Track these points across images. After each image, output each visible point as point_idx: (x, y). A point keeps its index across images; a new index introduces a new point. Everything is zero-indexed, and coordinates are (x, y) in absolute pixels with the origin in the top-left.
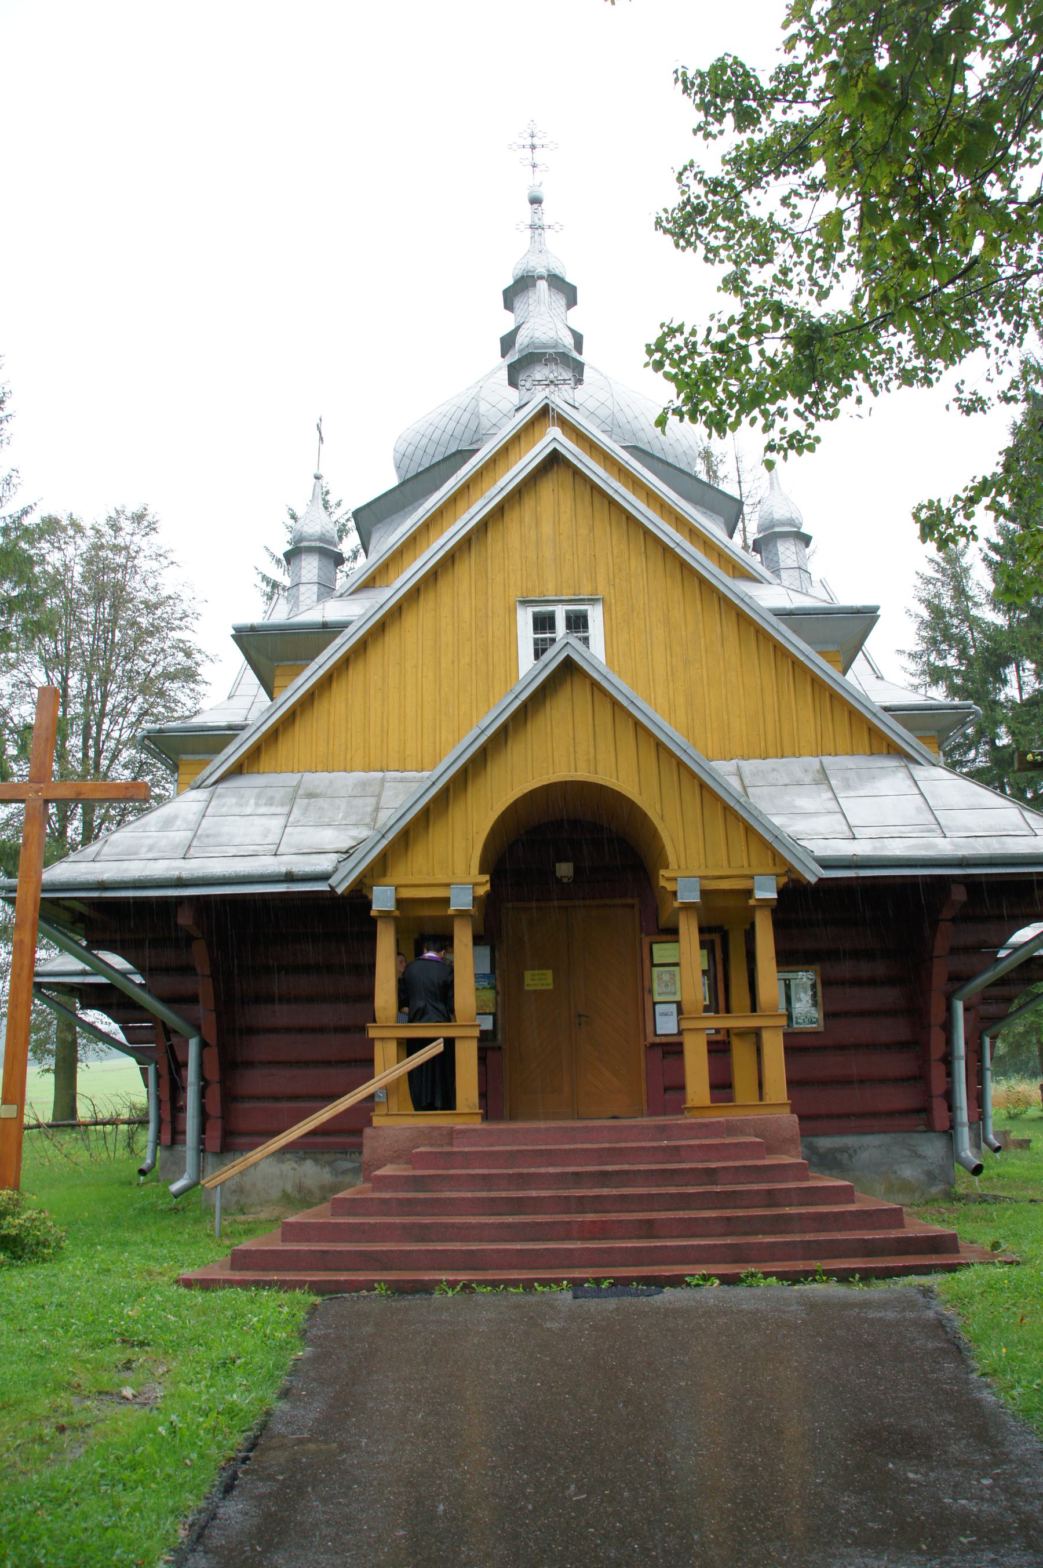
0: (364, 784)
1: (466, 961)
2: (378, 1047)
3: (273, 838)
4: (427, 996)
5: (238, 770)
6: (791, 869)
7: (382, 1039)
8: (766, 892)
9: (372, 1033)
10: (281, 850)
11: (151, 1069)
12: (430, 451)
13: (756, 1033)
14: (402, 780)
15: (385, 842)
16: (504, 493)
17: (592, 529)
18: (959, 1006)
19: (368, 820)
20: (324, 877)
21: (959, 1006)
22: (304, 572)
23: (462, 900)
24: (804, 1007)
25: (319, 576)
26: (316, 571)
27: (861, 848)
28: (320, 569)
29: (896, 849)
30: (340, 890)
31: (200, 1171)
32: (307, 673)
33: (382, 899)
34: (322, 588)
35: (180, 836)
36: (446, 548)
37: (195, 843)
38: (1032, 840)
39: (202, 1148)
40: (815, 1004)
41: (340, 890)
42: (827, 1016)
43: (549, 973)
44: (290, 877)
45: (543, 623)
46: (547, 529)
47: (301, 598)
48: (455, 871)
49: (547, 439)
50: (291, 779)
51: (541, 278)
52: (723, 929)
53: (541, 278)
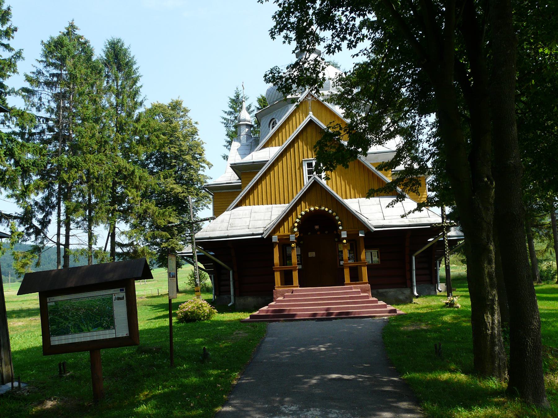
3: (248, 224)
11: (212, 276)
18: (414, 258)
20: (262, 234)
21: (414, 258)
23: (293, 238)
24: (376, 259)
32: (252, 181)
33: (275, 238)
35: (226, 225)
38: (429, 219)
43: (314, 253)
44: (253, 235)
48: (291, 231)
49: (309, 116)
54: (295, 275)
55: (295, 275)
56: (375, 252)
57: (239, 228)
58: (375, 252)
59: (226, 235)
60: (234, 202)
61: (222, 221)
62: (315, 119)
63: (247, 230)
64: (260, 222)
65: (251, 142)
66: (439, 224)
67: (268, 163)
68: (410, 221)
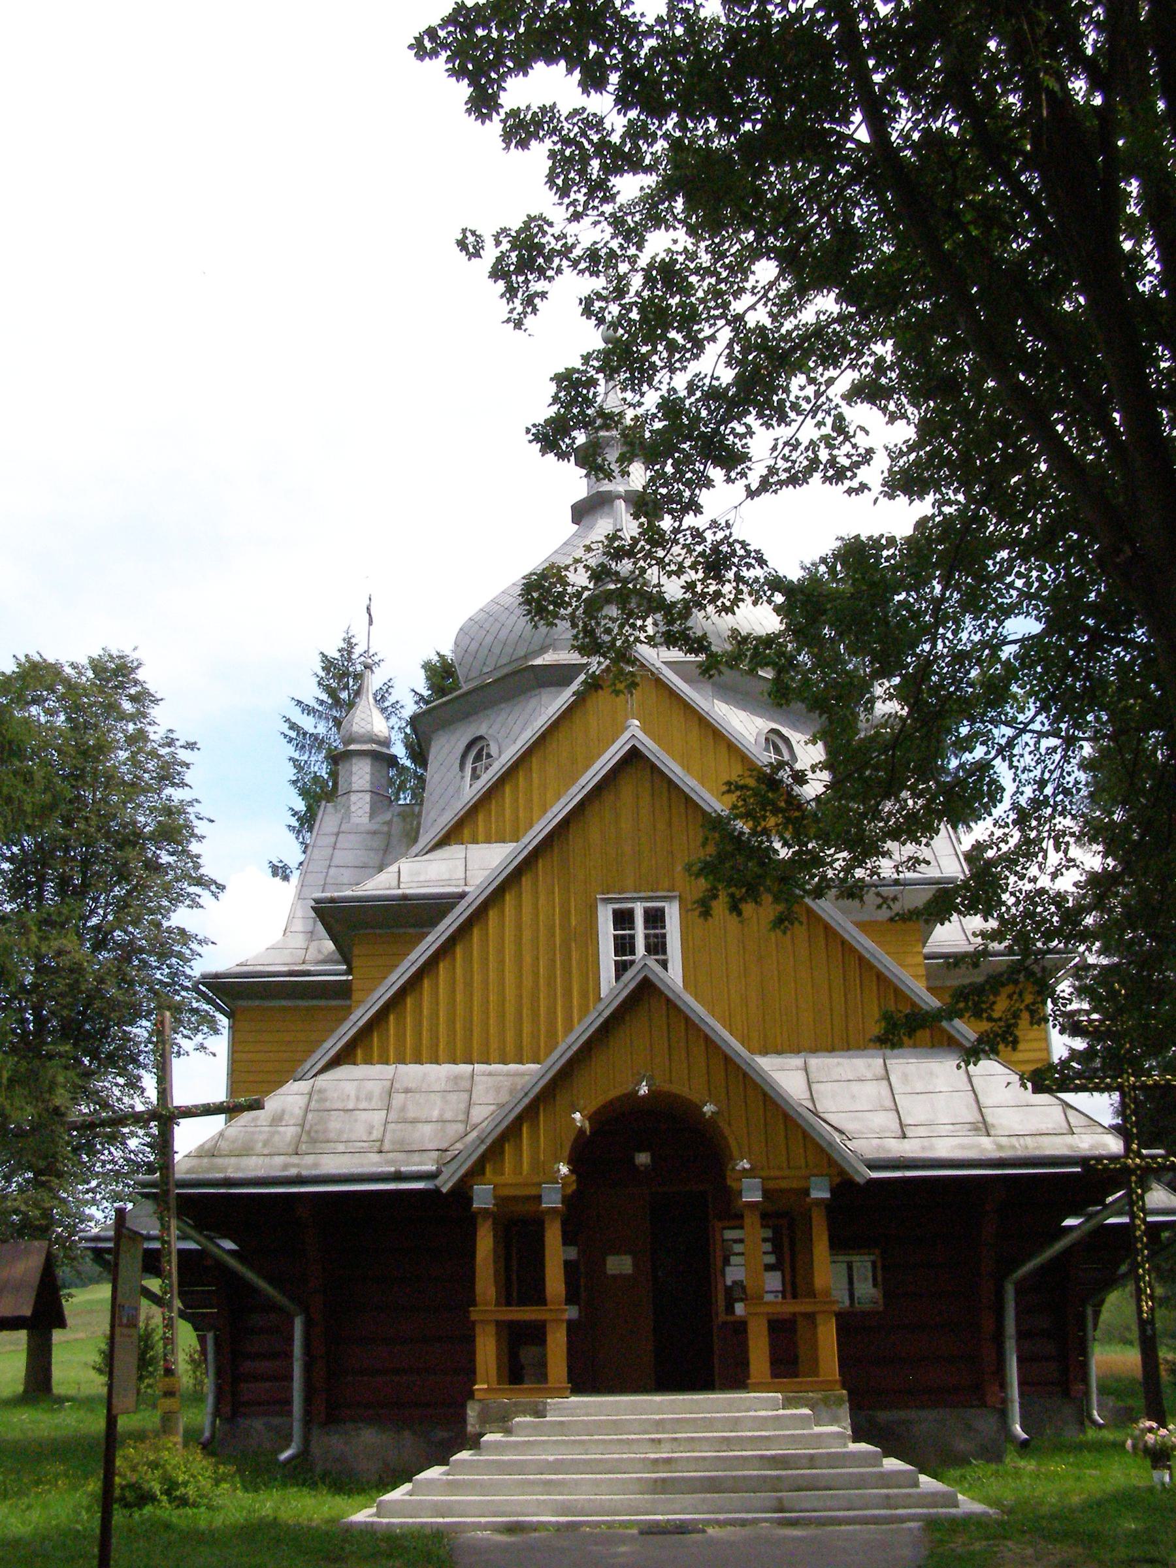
0: (456, 1078)
1: (556, 1253)
2: (478, 1330)
3: (376, 1134)
4: (523, 1282)
5: (336, 1062)
6: (842, 1172)
7: (482, 1321)
8: (820, 1192)
9: (473, 1317)
10: (387, 1146)
11: (210, 1336)
12: (497, 651)
13: (811, 1317)
14: (490, 1074)
15: (484, 1147)
16: (585, 791)
17: (670, 825)
19: (461, 1117)
22: (354, 778)
23: (552, 1200)
24: (866, 1290)
25: (372, 783)
26: (368, 777)
27: (909, 1149)
28: (372, 774)
29: (944, 1149)
30: (444, 1190)
31: (306, 1440)
32: (401, 969)
33: (483, 1196)
34: (375, 797)
36: (530, 848)
37: (304, 1138)
38: (1069, 1139)
39: (308, 1422)
40: (875, 1285)
41: (444, 1190)
42: (887, 1295)
44: (398, 1177)
45: (623, 919)
46: (626, 825)
47: (353, 808)
49: (627, 735)
50: (388, 1071)
51: (619, 497)
52: (785, 1222)
53: (619, 497)
54: (557, 1343)
55: (557, 1343)
56: (863, 1264)
57: (341, 1147)
58: (863, 1264)
59: (293, 1172)
60: (327, 1045)
61: (277, 1120)
62: (649, 746)
63: (375, 1157)
64: (427, 1129)
65: (389, 823)
66: (1113, 1158)
67: (464, 903)
68: (1000, 1147)
